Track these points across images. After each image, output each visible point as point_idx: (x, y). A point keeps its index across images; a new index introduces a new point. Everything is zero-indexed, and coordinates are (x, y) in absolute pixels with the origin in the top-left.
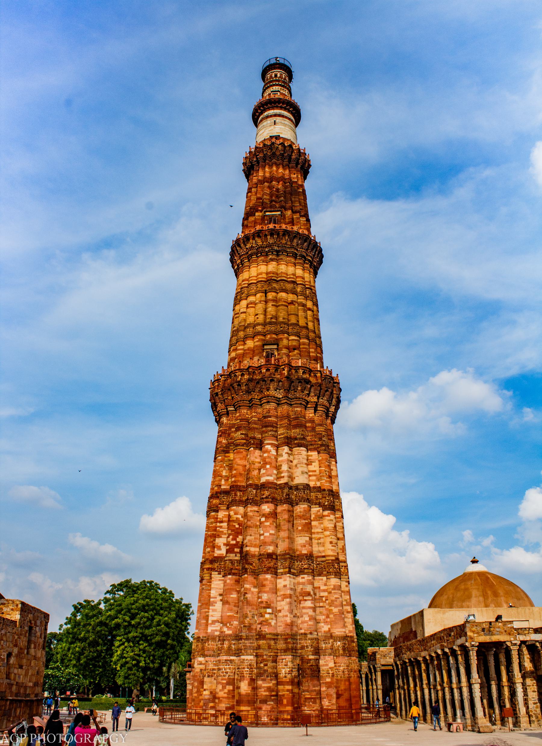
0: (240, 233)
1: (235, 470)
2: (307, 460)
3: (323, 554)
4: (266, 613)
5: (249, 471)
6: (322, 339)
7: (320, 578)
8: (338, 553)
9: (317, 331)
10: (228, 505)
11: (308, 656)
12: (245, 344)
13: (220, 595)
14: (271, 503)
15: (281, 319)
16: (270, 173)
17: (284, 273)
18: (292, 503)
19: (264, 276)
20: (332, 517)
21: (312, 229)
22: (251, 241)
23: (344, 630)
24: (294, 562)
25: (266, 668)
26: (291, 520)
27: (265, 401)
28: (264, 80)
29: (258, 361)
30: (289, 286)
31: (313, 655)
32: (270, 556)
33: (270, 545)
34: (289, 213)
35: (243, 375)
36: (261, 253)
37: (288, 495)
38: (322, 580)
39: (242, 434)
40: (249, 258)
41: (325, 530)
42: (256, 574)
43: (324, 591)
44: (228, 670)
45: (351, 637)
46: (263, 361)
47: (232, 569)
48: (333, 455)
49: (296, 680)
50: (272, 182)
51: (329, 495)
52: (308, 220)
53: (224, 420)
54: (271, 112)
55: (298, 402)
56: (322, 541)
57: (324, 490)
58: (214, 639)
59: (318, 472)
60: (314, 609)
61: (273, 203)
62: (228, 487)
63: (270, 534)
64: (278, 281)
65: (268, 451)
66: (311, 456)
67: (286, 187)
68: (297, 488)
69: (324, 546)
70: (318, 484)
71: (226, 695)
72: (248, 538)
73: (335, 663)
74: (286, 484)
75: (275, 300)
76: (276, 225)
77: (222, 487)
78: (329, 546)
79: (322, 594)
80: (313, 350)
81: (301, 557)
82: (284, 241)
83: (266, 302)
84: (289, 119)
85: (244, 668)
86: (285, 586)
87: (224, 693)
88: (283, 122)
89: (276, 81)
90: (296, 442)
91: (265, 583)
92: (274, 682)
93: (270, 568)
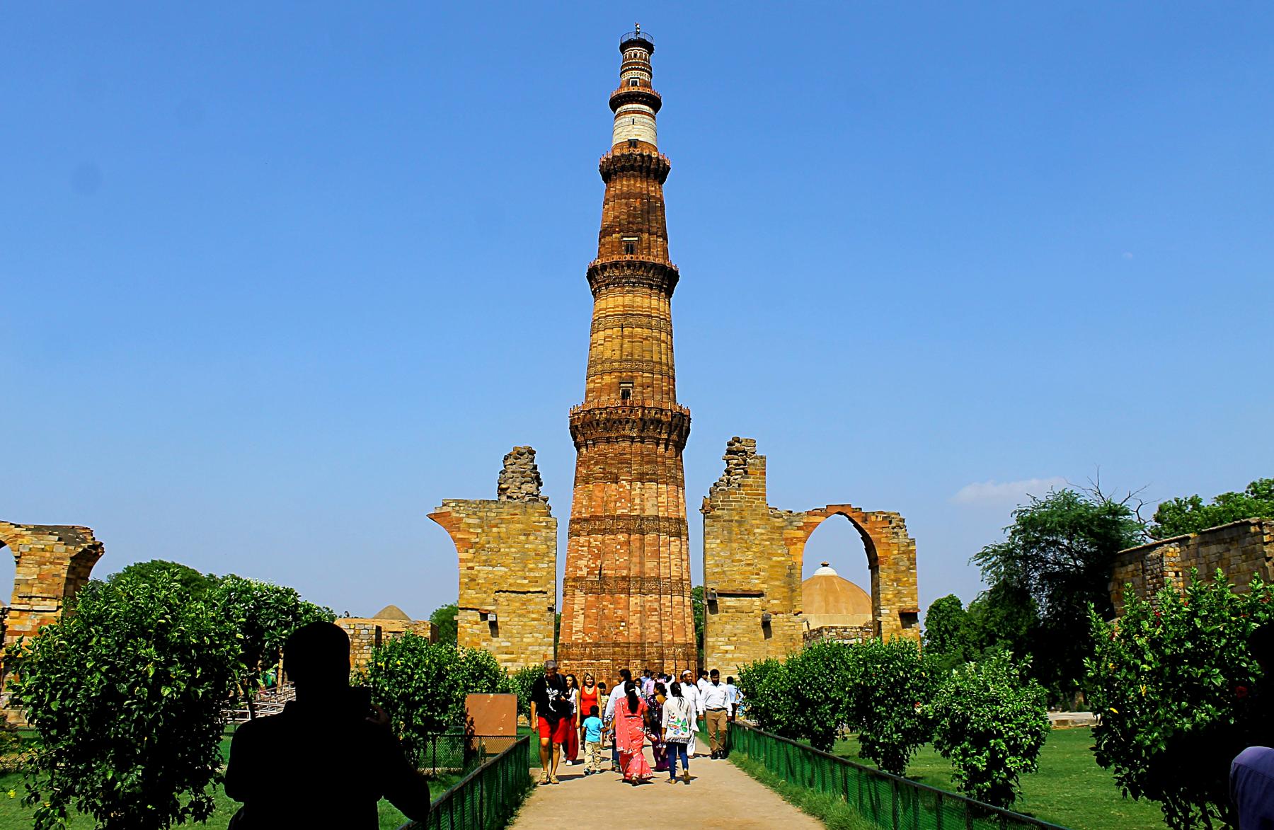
18: (642, 533)
24: (643, 584)
26: (642, 548)
29: (614, 400)
30: (645, 320)
32: (624, 578)
34: (646, 236)
36: (617, 282)
37: (637, 525)
42: (612, 593)
48: (680, 484)
53: (583, 450)
58: (577, 645)
81: (650, 579)
83: (622, 337)
84: (649, 114)
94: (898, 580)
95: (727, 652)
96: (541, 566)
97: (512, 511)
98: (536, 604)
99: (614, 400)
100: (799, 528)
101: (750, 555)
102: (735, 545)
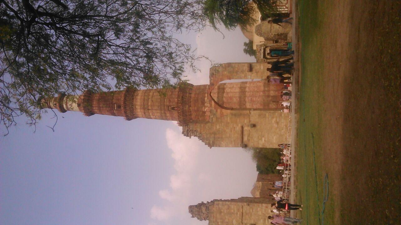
12: (168, 116)
15: (159, 105)
16: (95, 107)
19: (142, 110)
20: (227, 89)
40: (134, 115)
43: (250, 93)
50: (100, 107)
54: (64, 106)
60: (256, 97)
61: (110, 106)
65: (207, 111)
70: (216, 94)
75: (151, 106)
76: (122, 106)
83: (152, 109)
94: (237, 72)
95: (265, 140)
100: (217, 111)
101: (227, 130)
102: (224, 136)
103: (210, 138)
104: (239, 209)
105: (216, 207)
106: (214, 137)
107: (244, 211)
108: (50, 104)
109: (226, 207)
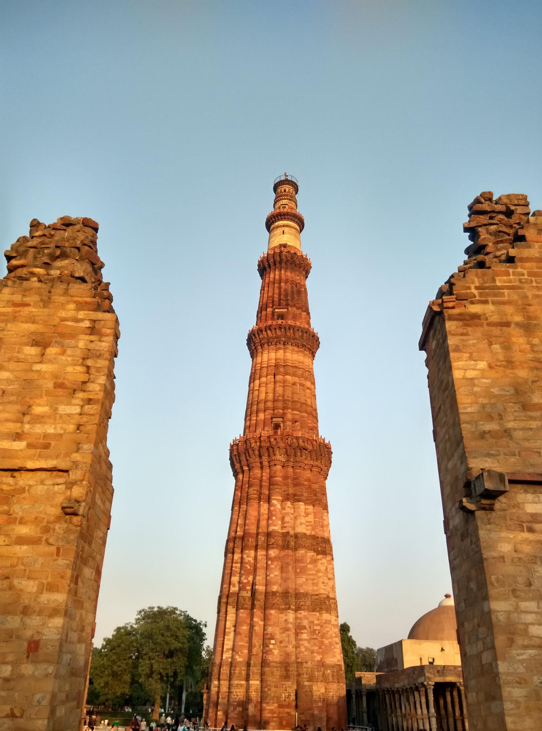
0: (255, 326)
1: (248, 520)
2: (305, 512)
3: (317, 593)
4: (270, 644)
5: (258, 521)
6: (318, 411)
7: (314, 613)
8: (328, 592)
9: (313, 406)
10: (242, 549)
11: (303, 682)
12: (257, 416)
13: (235, 626)
14: (276, 548)
15: (286, 398)
16: (280, 275)
17: (289, 360)
19: (274, 361)
20: (324, 561)
21: (312, 321)
22: (264, 333)
23: (333, 660)
25: (269, 692)
27: (272, 464)
28: (275, 193)
29: (268, 431)
31: (307, 681)
32: (274, 593)
33: (274, 585)
34: (294, 309)
35: (256, 442)
38: (315, 615)
39: (254, 490)
40: (262, 345)
41: (318, 572)
43: (317, 625)
44: (238, 694)
45: (340, 665)
46: (271, 432)
47: (244, 604)
49: (294, 704)
50: (280, 283)
51: (322, 542)
52: (308, 314)
54: (281, 223)
55: (298, 465)
56: (315, 581)
57: (318, 537)
59: (313, 523)
60: (309, 641)
62: (242, 534)
63: (275, 575)
64: (284, 366)
66: (308, 509)
67: (292, 287)
68: (296, 536)
69: (317, 586)
70: (313, 533)
71: (236, 716)
72: (258, 578)
73: (326, 689)
74: (288, 533)
77: (238, 533)
78: (322, 586)
79: (316, 628)
80: (310, 422)
82: (288, 334)
83: (275, 382)
84: (295, 229)
85: (252, 692)
86: (286, 620)
87: (235, 714)
88: (290, 231)
89: (286, 195)
90: (296, 498)
91: (269, 617)
92: (276, 705)
93: (274, 604)
96: (64, 409)
97: (17, 298)
98: (35, 500)
99: (268, 431)
103: (493, 303)
104: (47, 446)
105: (77, 320)
106: (507, 324)
107: (24, 480)
108: (285, 199)
109: (74, 372)
